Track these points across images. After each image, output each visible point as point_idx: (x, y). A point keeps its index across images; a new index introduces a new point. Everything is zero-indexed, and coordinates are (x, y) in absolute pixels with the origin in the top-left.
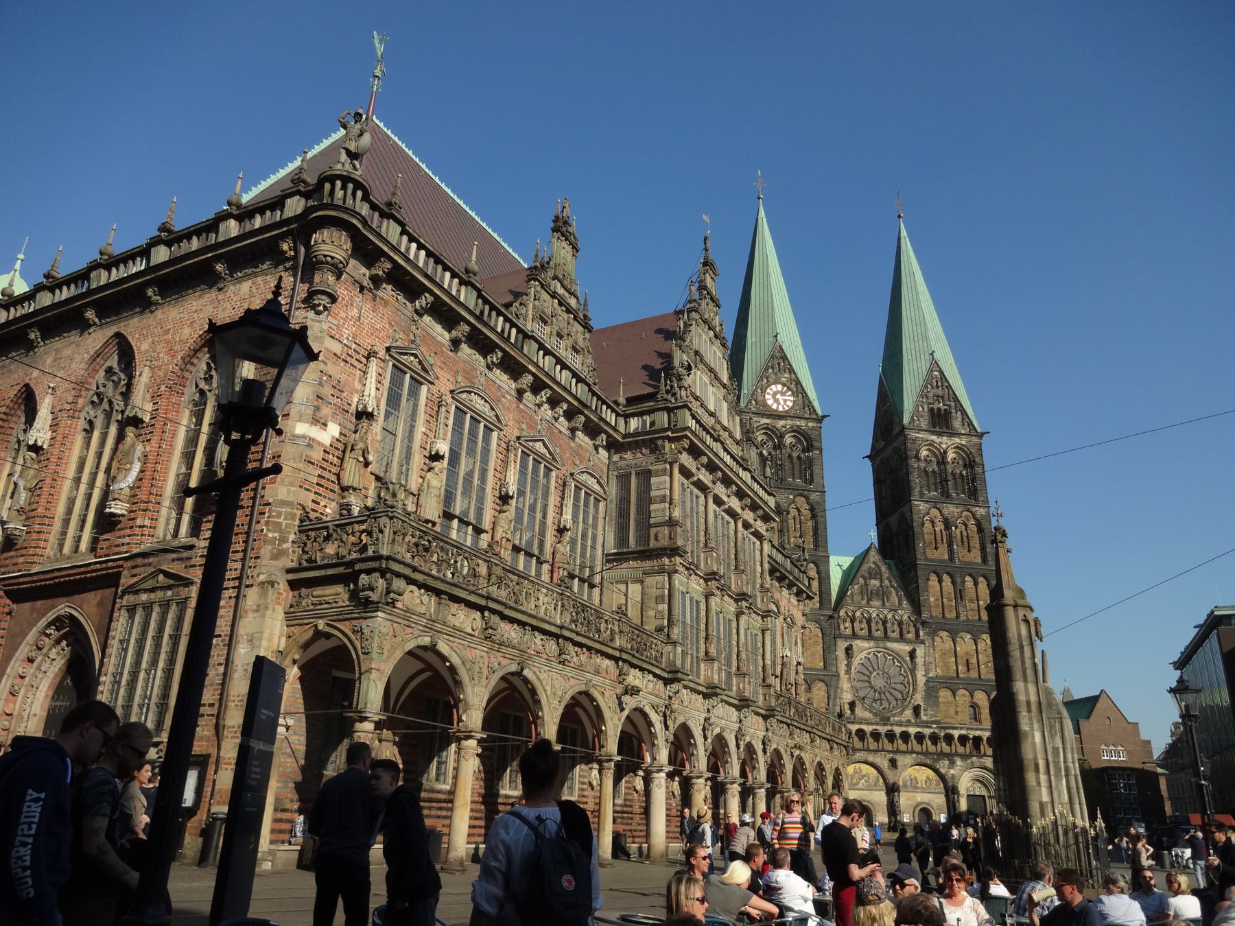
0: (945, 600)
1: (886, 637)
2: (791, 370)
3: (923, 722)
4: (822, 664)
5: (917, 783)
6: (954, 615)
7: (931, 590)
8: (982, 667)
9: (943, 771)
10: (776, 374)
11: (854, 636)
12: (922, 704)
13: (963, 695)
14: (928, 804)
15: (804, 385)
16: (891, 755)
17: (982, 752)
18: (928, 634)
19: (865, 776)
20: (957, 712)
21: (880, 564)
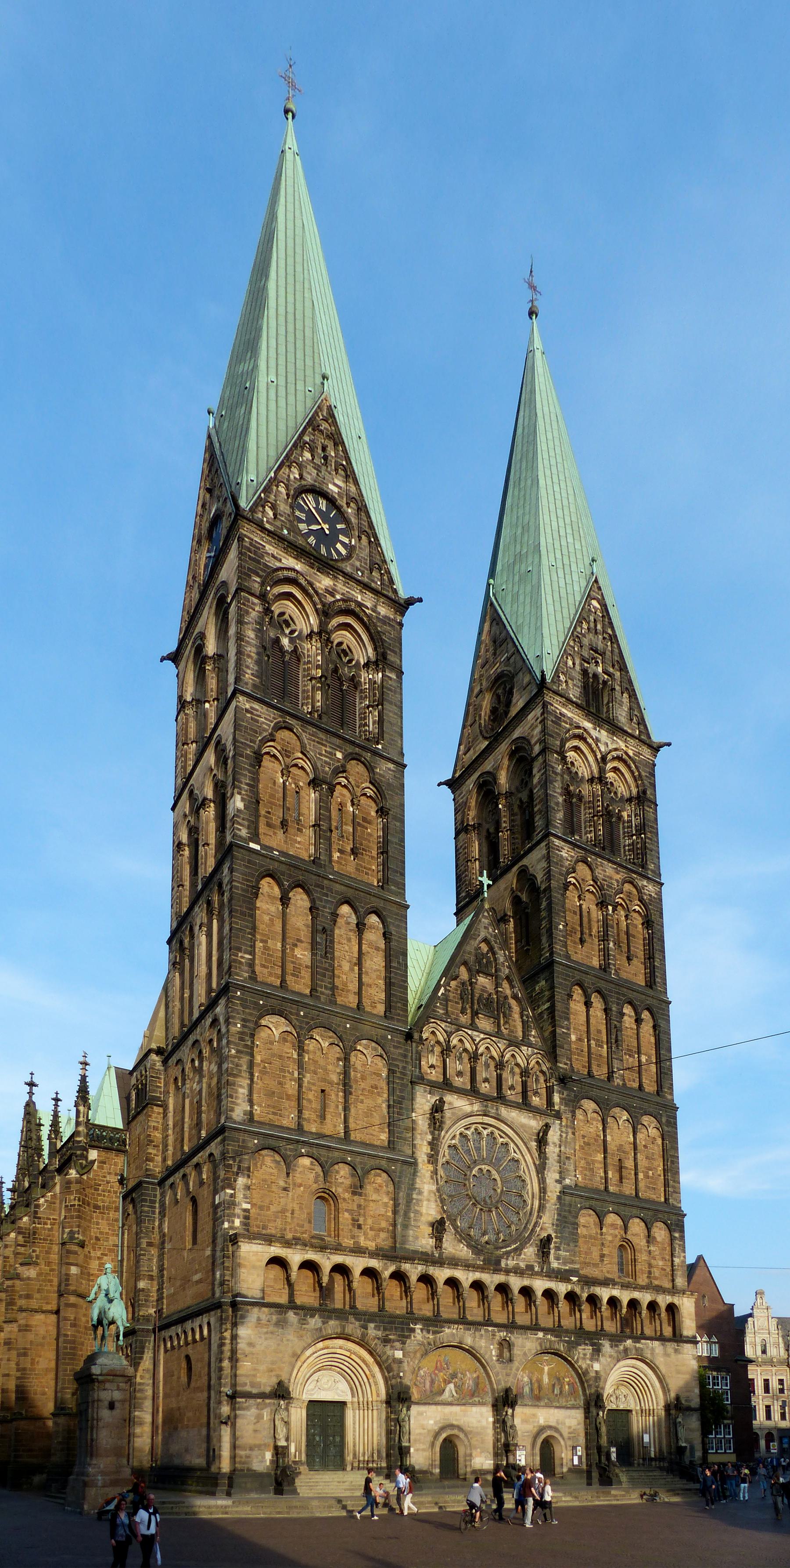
1: (500, 1098)
4: (384, 1137)
9: (583, 1364)
11: (446, 1085)
12: (553, 1235)
13: (613, 1226)
14: (556, 1430)
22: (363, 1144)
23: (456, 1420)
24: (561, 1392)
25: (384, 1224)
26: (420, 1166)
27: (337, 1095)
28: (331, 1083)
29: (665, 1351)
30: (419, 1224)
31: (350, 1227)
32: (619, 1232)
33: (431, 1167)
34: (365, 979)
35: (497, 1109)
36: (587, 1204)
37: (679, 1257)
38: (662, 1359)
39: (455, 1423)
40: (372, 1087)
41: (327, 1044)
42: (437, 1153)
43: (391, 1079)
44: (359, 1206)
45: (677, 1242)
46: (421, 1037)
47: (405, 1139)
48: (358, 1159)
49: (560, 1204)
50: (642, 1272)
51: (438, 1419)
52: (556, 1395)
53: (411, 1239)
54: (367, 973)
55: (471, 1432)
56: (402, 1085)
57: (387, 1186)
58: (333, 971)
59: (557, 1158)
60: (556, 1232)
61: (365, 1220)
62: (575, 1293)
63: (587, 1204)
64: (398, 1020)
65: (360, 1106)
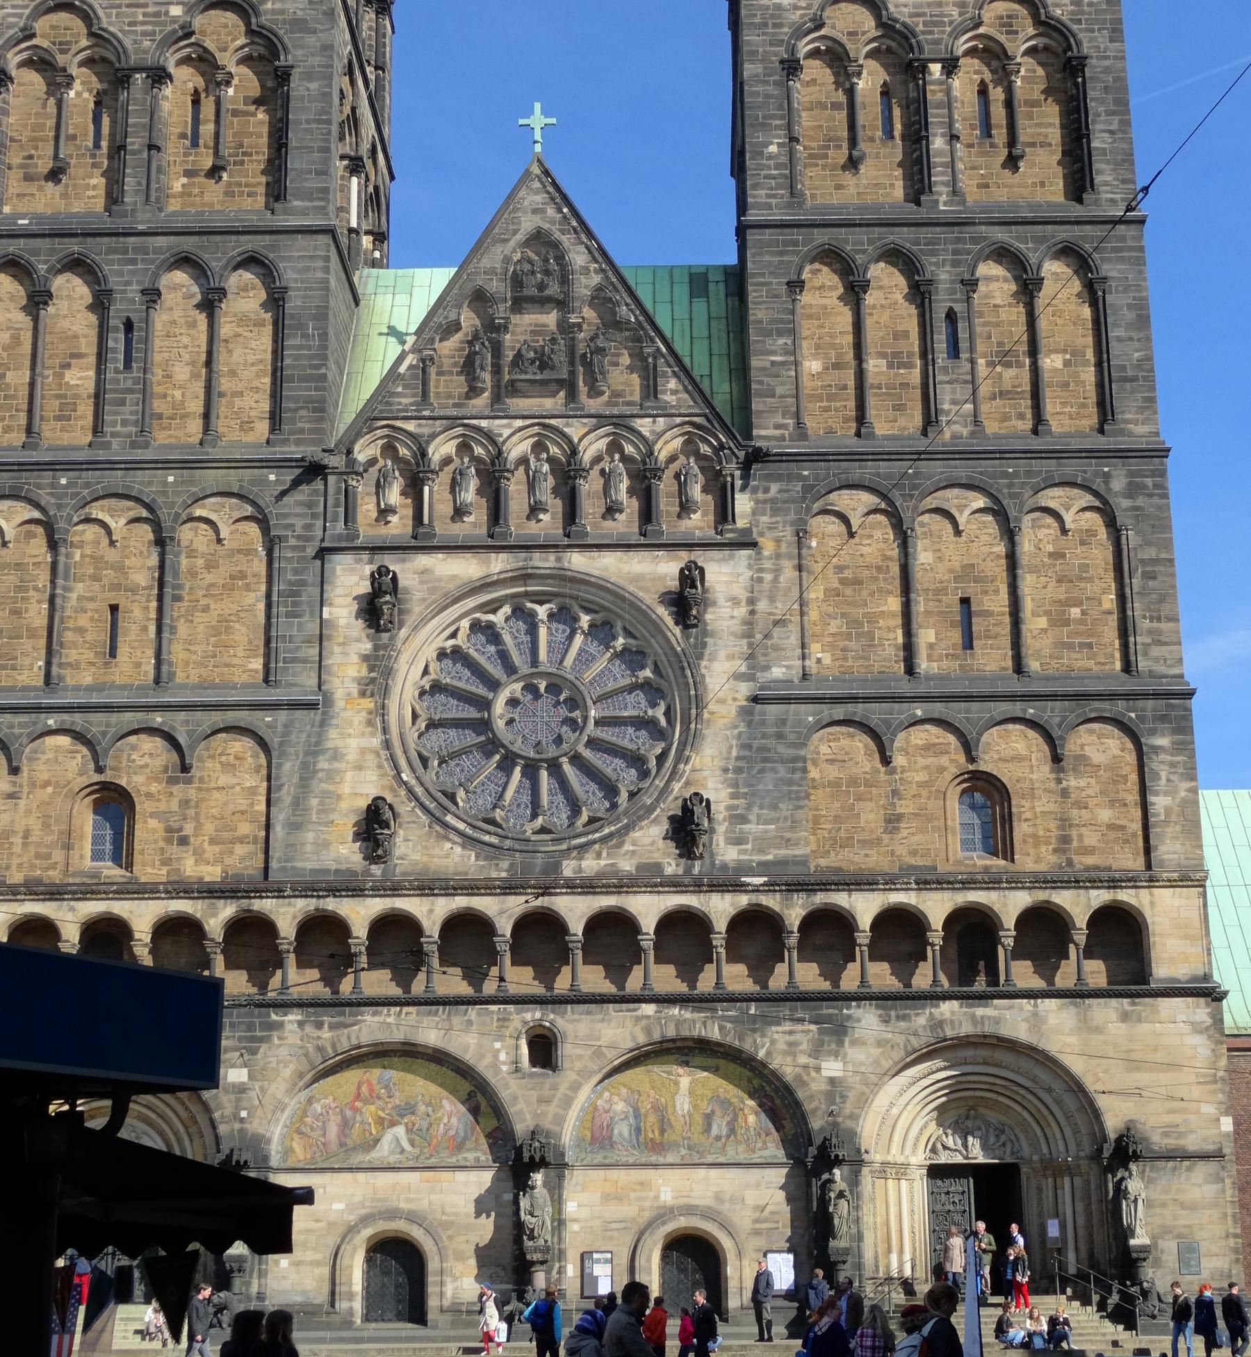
0: (874, 365)
3: (724, 867)
4: (257, 664)
5: (664, 1125)
6: (915, 419)
7: (807, 328)
8: (1034, 623)
13: (928, 748)
14: (707, 1214)
17: (1002, 981)
18: (776, 507)
20: (893, 821)
21: (566, 240)
22: (202, 686)
23: (408, 1200)
24: (732, 1131)
25: (245, 829)
26: (340, 703)
27: (147, 608)
28: (134, 590)
30: (332, 817)
31: (161, 844)
32: (954, 760)
33: (368, 704)
34: (224, 384)
35: (559, 560)
36: (839, 712)
37: (1171, 792)
39: (403, 1205)
40: (232, 577)
41: (123, 521)
42: (388, 673)
43: (276, 554)
44: (185, 803)
45: (1163, 757)
46: (351, 462)
47: (304, 661)
48: (182, 716)
49: (749, 724)
51: (357, 1199)
52: (718, 1138)
53: (309, 848)
54: (233, 373)
55: (451, 1223)
56: (300, 560)
57: (256, 756)
58: (144, 391)
59: (738, 628)
60: (736, 785)
61: (198, 827)
63: (839, 712)
64: (298, 442)
65: (199, 617)
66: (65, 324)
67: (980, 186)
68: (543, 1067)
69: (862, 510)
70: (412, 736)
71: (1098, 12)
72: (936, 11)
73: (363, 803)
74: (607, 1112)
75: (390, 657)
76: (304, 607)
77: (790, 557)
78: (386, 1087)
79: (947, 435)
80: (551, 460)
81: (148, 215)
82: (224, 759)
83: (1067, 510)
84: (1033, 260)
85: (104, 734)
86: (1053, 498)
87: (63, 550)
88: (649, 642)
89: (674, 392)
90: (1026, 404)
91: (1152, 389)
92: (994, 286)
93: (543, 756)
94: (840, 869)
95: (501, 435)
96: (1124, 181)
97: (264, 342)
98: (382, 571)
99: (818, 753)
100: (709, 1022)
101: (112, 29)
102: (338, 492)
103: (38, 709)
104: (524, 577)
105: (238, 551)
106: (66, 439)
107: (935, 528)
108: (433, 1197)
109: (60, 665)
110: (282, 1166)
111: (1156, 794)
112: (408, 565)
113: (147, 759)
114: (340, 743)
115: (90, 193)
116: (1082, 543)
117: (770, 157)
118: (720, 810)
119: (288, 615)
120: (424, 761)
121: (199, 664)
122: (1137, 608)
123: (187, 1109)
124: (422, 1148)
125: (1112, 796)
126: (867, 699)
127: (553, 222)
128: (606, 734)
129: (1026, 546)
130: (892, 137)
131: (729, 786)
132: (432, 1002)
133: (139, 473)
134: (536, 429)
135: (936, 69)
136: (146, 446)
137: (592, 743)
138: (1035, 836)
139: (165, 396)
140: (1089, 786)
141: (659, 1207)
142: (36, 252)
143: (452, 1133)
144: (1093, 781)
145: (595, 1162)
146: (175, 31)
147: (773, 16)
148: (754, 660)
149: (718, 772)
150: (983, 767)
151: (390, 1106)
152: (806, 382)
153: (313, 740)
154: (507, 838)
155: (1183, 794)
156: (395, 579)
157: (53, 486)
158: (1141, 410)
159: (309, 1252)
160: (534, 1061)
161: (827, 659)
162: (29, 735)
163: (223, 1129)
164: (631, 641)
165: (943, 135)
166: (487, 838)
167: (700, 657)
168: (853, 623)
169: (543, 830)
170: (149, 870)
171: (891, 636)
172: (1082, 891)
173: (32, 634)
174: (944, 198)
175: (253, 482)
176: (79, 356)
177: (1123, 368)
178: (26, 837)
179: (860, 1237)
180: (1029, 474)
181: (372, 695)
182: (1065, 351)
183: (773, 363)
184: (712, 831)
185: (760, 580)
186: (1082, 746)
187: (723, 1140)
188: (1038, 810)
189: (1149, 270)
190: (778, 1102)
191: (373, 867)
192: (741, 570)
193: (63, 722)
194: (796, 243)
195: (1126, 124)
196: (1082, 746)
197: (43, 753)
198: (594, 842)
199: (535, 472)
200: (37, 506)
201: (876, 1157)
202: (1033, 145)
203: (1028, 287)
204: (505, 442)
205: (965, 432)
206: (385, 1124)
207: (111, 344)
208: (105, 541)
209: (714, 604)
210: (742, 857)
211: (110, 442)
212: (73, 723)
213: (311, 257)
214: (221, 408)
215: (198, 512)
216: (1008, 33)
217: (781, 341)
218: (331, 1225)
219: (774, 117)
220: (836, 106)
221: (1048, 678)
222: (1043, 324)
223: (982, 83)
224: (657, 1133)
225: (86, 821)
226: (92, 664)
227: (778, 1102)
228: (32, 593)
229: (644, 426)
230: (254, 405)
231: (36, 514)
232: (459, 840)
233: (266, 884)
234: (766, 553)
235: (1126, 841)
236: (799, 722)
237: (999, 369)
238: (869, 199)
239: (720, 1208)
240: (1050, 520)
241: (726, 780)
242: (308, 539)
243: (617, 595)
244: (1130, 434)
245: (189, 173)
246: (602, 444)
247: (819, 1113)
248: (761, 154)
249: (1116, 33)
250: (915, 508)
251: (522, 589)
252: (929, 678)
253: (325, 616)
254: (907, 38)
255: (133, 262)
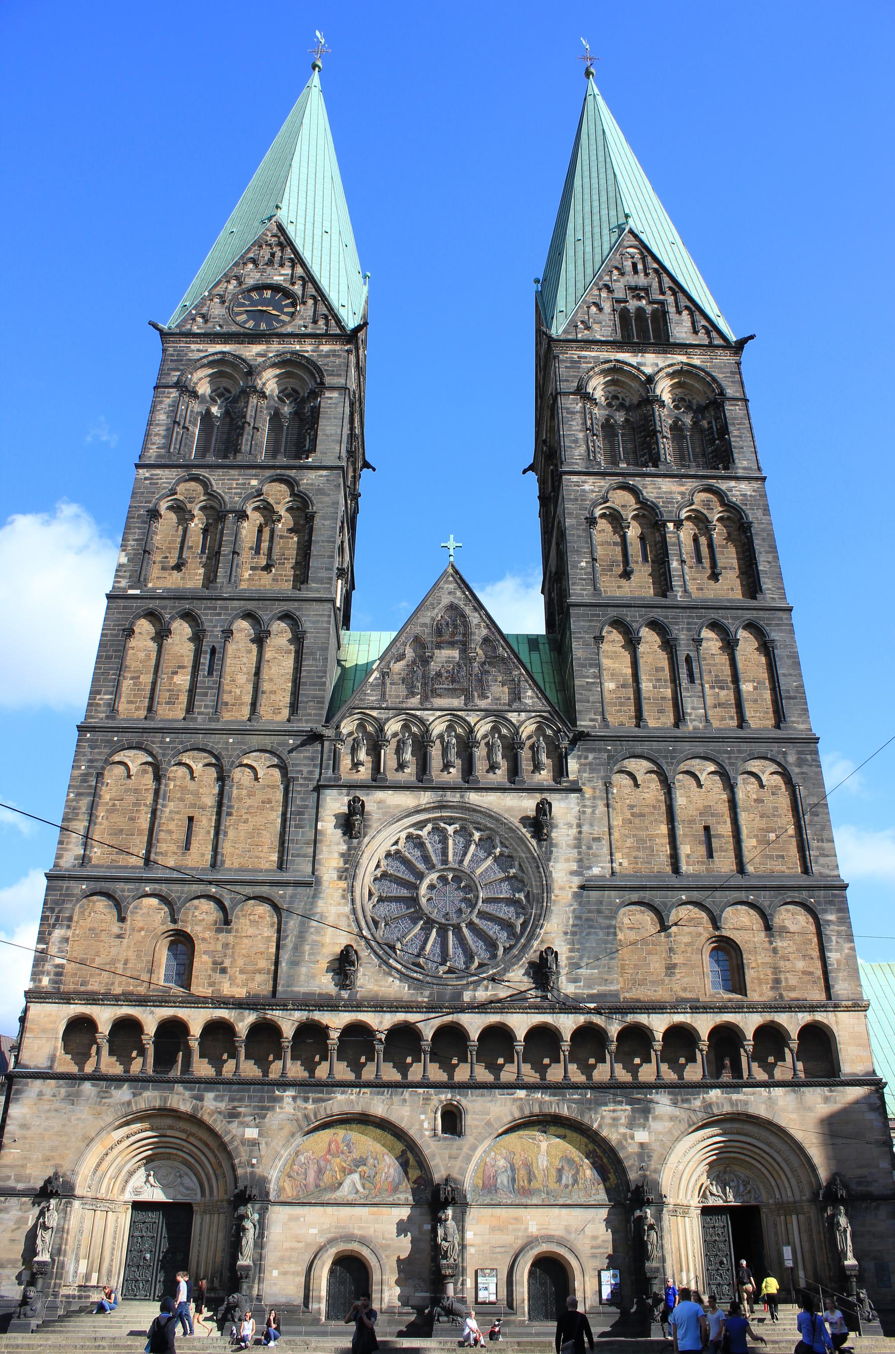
2: (297, 260)
4: (275, 857)
5: (531, 1176)
8: (749, 843)
9: (612, 1135)
10: (263, 272)
12: (562, 949)
15: (324, 283)
16: (446, 1096)
17: (745, 1075)
18: (592, 768)
19: (362, 1162)
20: (671, 968)
21: (468, 610)
23: (360, 1228)
24: (576, 1181)
27: (210, 819)
28: (203, 808)
29: (801, 1102)
30: (318, 958)
31: (210, 972)
32: (705, 929)
33: (343, 884)
35: (462, 797)
36: (635, 896)
38: (794, 1116)
39: (356, 1232)
40: (263, 802)
41: (200, 765)
42: (357, 865)
44: (226, 946)
45: (832, 927)
49: (580, 904)
50: (760, 982)
51: (325, 1227)
52: (567, 1186)
53: (302, 978)
59: (572, 842)
62: (597, 1025)
63: (635, 896)
64: (307, 721)
65: (242, 826)
66: (177, 648)
67: (698, 589)
68: (452, 1134)
69: (643, 771)
70: (369, 906)
71: (755, 500)
72: (669, 496)
73: (338, 950)
74: (493, 1166)
75: (357, 854)
76: (306, 822)
77: (602, 799)
78: (347, 1145)
79: (691, 728)
80: (457, 736)
81: (229, 590)
82: (252, 917)
83: (763, 773)
84: (732, 630)
85: (179, 898)
86: (755, 766)
87: (163, 781)
88: (516, 850)
89: (532, 698)
90: (733, 711)
91: (806, 703)
92: (711, 643)
93: (450, 922)
94: (638, 1001)
95: (428, 720)
96: (778, 588)
97: (289, 663)
98: (356, 800)
99: (623, 923)
100: (561, 1104)
101: (218, 491)
102: (330, 752)
103: (140, 880)
104: (441, 807)
105: (268, 786)
106: (171, 715)
107: (686, 783)
108: (376, 1226)
109: (156, 853)
110: (277, 1200)
111: (830, 951)
112: (370, 797)
113: (204, 916)
114: (325, 910)
115: (198, 577)
116: (773, 794)
117: (582, 569)
118: (563, 960)
119: (296, 826)
120: (376, 923)
121: (239, 856)
122: (809, 833)
123: (216, 1156)
124: (370, 1190)
125: (804, 953)
126: (652, 888)
127: (460, 599)
128: (490, 908)
129: (740, 795)
130: (648, 561)
131: (568, 944)
132: (378, 1085)
133: (214, 736)
134: (449, 717)
135: (671, 525)
136: (218, 720)
137: (482, 915)
138: (759, 979)
139: (230, 692)
140: (789, 946)
141: (527, 1237)
142: (164, 608)
143: (390, 1179)
144: (791, 943)
145: (486, 1202)
146: (252, 493)
147: (580, 495)
148: (583, 864)
149: (561, 935)
150: (725, 933)
151: (349, 1159)
152: (606, 694)
153: (308, 907)
154: (428, 975)
155: (846, 951)
156: (363, 805)
157: (161, 742)
158: (800, 716)
159: (293, 1265)
160: (444, 1131)
161: (625, 863)
162: (133, 897)
163: (240, 1171)
164: (504, 849)
165: (677, 560)
166: (415, 975)
167: (549, 860)
168: (641, 840)
169: (450, 971)
170: (201, 989)
171: (664, 849)
172: (793, 1014)
173: (140, 833)
174: (680, 594)
175: (279, 744)
176: (183, 667)
177: (788, 691)
178: (125, 964)
179: (663, 1260)
180: (739, 752)
181: (346, 879)
182: (754, 681)
183: (587, 682)
184: (558, 973)
185: (584, 812)
186: (783, 920)
187: (570, 1187)
188: (759, 961)
189: (796, 636)
190: (605, 1160)
191: (343, 992)
192: (572, 806)
193: (155, 889)
194: (598, 616)
195: (777, 558)
196: (783, 920)
197: (141, 909)
198: (484, 979)
199: (448, 743)
200: (151, 754)
201: (670, 1200)
202: (725, 568)
203: (730, 645)
204: (430, 724)
205: (701, 726)
206: (347, 1172)
207: (202, 660)
208: (189, 777)
209: (557, 826)
210: (578, 991)
211: (196, 718)
212: (161, 890)
213: (320, 615)
214: (263, 700)
215: (245, 762)
216: (708, 509)
217: (592, 670)
218: (308, 1245)
219: (582, 547)
220: (615, 544)
221: (760, 877)
222: (740, 666)
223: (695, 534)
224: (526, 1182)
225: (163, 955)
226: (175, 853)
227: (605, 1160)
228: (142, 807)
229: (513, 717)
230: (282, 699)
231: (150, 759)
232: (398, 976)
233: (274, 1000)
234: (587, 796)
235: (815, 982)
236: (610, 903)
237: (717, 690)
238: (636, 594)
239: (568, 1237)
240: (753, 780)
241: (566, 939)
242: (310, 780)
243: (497, 820)
244: (795, 729)
245: (253, 568)
246: (488, 727)
247: (634, 1168)
248: (577, 567)
249: (766, 511)
250: (675, 770)
251: (439, 815)
252: (689, 876)
253: (319, 827)
254: (654, 510)
255: (219, 614)
